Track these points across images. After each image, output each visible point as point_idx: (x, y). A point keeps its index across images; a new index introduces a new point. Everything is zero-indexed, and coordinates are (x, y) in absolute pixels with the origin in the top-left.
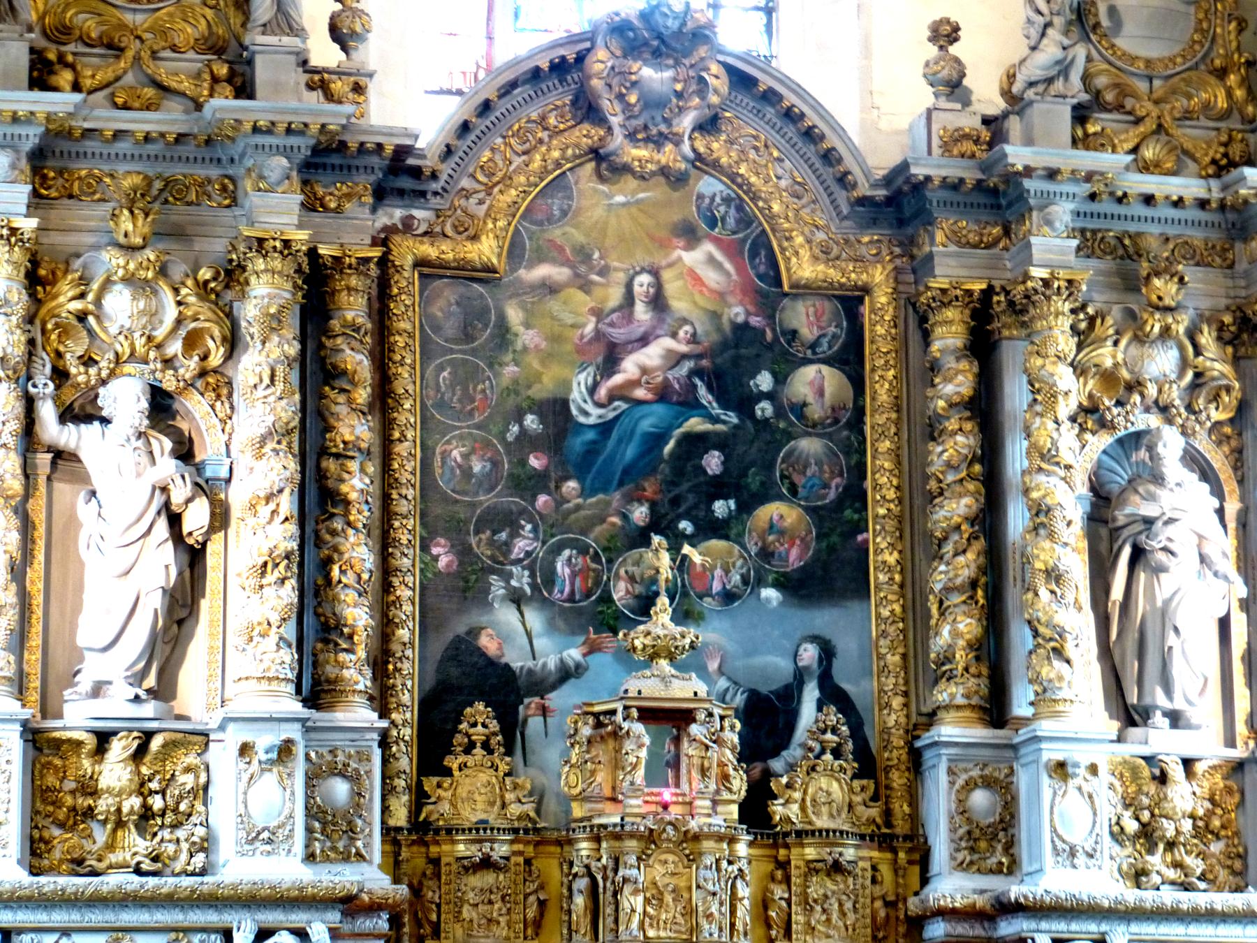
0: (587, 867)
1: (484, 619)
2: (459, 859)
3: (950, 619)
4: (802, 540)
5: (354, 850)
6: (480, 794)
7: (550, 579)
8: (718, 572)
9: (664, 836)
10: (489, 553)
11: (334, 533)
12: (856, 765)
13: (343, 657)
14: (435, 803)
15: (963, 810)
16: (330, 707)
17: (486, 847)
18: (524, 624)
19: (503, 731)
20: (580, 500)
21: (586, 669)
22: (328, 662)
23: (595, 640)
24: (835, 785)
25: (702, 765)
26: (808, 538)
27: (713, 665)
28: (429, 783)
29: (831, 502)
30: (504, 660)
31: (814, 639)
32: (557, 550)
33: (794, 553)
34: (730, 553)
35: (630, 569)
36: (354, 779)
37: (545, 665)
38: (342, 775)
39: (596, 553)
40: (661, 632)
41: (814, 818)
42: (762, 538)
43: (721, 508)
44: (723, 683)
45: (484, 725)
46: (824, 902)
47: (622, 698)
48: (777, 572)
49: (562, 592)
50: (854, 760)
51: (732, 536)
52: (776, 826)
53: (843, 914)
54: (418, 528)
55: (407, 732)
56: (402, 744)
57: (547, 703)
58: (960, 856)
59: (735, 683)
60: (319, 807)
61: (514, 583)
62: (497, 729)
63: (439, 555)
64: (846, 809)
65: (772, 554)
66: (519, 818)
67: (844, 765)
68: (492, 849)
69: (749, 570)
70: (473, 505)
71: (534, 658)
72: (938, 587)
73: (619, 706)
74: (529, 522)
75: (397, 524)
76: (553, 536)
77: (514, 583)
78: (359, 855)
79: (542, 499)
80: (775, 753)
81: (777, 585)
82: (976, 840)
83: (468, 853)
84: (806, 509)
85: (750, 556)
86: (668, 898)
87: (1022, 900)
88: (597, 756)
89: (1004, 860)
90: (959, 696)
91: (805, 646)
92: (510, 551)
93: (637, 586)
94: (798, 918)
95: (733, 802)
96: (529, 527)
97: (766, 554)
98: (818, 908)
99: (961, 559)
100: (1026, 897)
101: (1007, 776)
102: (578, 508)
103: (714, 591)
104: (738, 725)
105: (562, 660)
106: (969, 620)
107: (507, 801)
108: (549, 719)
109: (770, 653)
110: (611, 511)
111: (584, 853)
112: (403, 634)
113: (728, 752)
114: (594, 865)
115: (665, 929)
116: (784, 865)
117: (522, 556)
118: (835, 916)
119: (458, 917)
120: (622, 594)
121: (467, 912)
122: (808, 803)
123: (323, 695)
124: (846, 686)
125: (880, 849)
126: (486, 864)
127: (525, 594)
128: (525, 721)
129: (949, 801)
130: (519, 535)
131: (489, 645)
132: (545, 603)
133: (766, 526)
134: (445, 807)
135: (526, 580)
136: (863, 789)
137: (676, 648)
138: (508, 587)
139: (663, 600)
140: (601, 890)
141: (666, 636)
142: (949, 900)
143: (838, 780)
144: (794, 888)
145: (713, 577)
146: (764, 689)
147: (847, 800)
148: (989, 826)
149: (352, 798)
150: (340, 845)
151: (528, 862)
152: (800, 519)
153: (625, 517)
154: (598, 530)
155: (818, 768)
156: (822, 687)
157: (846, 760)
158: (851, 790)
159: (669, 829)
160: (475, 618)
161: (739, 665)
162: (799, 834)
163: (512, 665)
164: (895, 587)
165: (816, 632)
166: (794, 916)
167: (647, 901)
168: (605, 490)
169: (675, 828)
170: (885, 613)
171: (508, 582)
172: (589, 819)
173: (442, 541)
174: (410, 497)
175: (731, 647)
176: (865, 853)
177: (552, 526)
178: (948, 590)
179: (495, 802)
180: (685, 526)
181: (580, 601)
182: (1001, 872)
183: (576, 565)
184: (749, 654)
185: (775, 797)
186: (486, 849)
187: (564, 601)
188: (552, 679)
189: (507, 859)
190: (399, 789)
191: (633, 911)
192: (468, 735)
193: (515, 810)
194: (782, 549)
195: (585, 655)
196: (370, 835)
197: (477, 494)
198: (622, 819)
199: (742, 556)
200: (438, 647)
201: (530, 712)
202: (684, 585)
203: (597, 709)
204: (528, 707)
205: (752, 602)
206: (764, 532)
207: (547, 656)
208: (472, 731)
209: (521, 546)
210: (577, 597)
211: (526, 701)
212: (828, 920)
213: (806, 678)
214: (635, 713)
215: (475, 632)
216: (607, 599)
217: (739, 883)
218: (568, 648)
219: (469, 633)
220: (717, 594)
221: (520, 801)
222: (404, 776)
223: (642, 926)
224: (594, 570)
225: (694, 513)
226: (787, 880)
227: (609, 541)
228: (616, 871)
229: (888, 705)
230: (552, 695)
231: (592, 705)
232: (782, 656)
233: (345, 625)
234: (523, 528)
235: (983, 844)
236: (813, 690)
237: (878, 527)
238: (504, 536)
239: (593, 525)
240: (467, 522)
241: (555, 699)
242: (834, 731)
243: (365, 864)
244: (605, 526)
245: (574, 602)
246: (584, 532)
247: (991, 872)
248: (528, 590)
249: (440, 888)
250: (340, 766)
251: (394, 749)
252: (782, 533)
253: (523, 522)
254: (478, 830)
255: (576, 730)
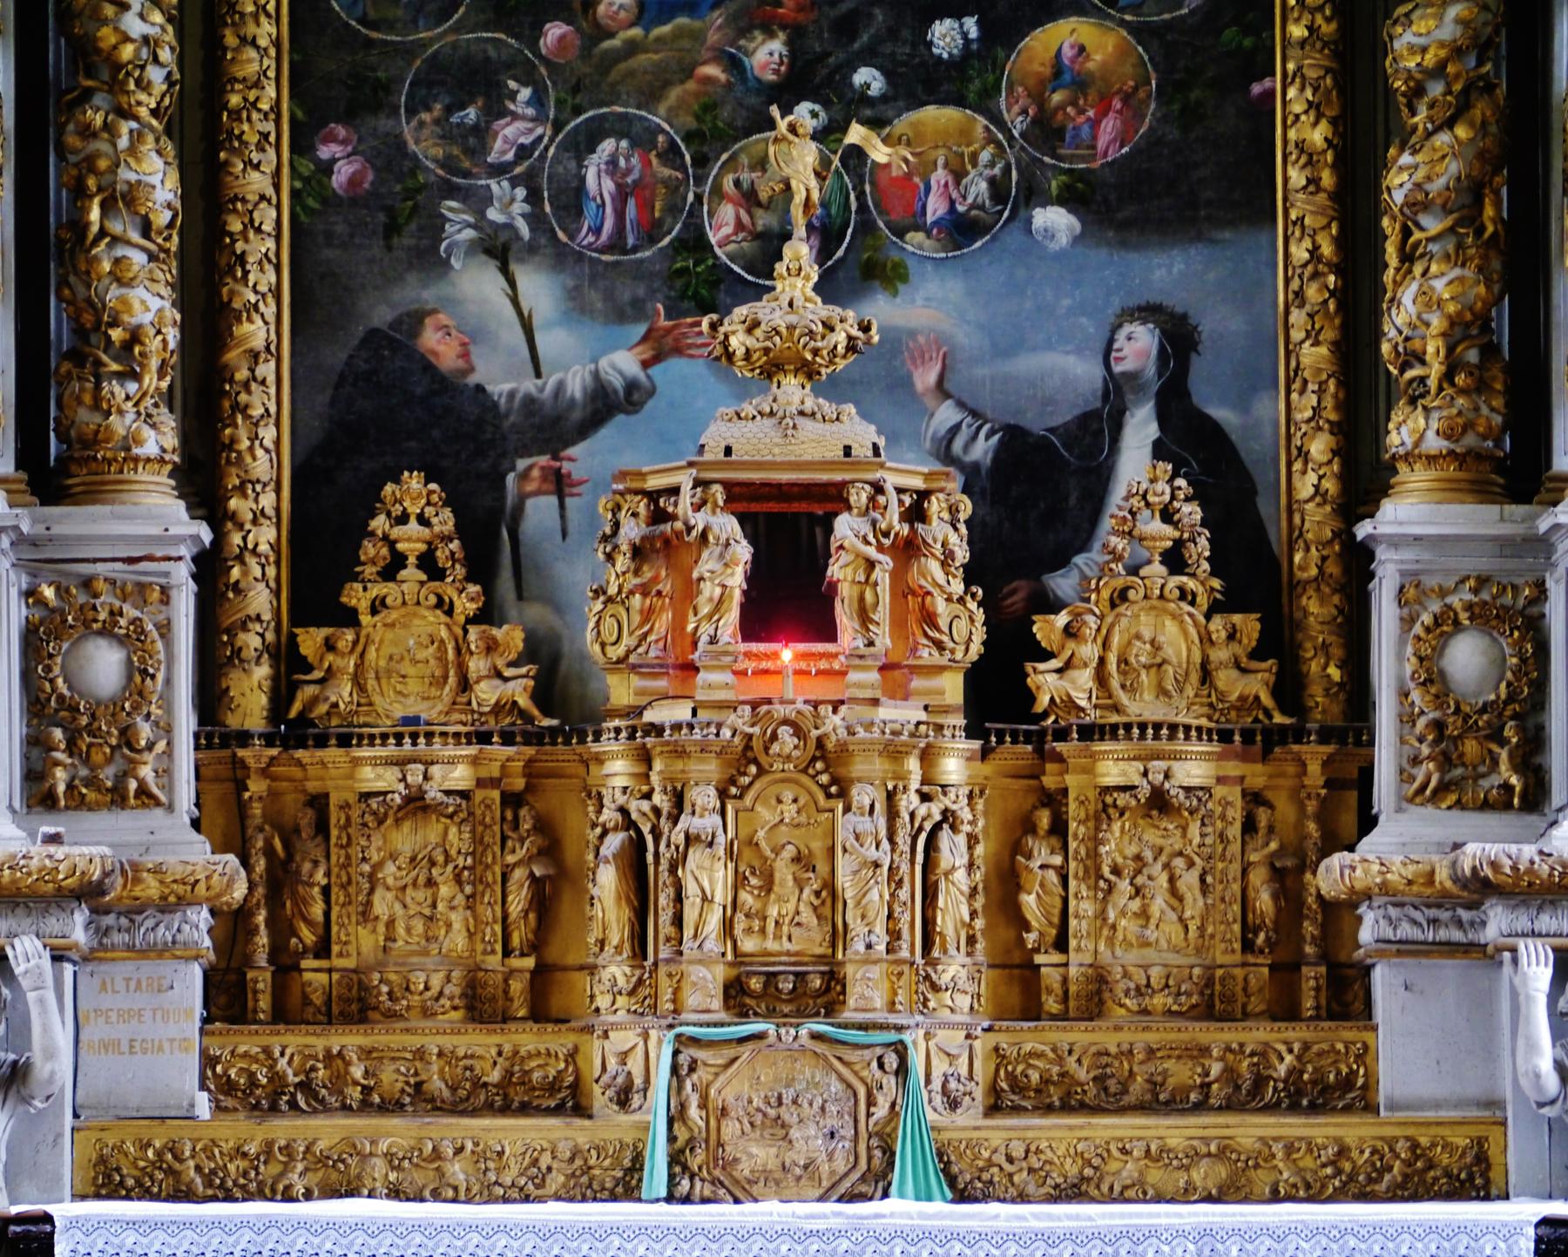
0: (623, 811)
1: (429, 295)
2: (366, 796)
3: (1418, 269)
4: (1127, 99)
5: (133, 785)
6: (415, 662)
7: (572, 199)
8: (940, 176)
9: (775, 748)
10: (439, 152)
11: (87, 132)
12: (1216, 583)
13: (117, 391)
14: (321, 682)
15: (1433, 677)
16: (92, 494)
17: (415, 774)
18: (515, 301)
19: (461, 530)
20: (636, 32)
21: (652, 392)
22: (79, 401)
23: (668, 331)
24: (1171, 627)
25: (862, 599)
26: (1142, 94)
27: (925, 378)
28: (310, 641)
29: (1192, 12)
30: (473, 379)
31: (1148, 312)
32: (584, 143)
33: (1109, 127)
34: (965, 134)
35: (746, 177)
36: (134, 639)
37: (560, 387)
38: (107, 632)
39: (673, 145)
40: (780, 320)
41: (1124, 698)
42: (1039, 99)
43: (946, 36)
44: (947, 415)
45: (423, 520)
46: (1138, 872)
47: (691, 464)
48: (1070, 171)
49: (597, 231)
50: (1213, 574)
51: (972, 96)
52: (1045, 715)
53: (1174, 891)
54: (285, 106)
55: (265, 536)
56: (252, 561)
57: (566, 466)
58: (1420, 774)
59: (975, 414)
60: (61, 698)
61: (493, 214)
62: (450, 526)
63: (334, 161)
64: (1195, 677)
65: (1060, 133)
66: (498, 709)
67: (1191, 584)
68: (426, 777)
69: (1007, 170)
70: (409, 51)
71: (538, 375)
72: (1399, 197)
73: (685, 480)
74: (525, 84)
75: (235, 100)
76: (577, 111)
77: (493, 214)
78: (143, 792)
79: (554, 31)
80: (1061, 561)
81: (1069, 199)
82: (1456, 740)
83: (380, 785)
84: (1137, 31)
85: (1011, 138)
86: (784, 872)
87: (1488, 871)
88: (655, 580)
89: (1514, 780)
90: (1431, 434)
91: (1127, 329)
92: (485, 149)
93: (759, 212)
94: (1083, 907)
95: (940, 669)
96: (525, 93)
97: (1047, 131)
98: (1124, 886)
99: (1443, 139)
100: (1494, 865)
101: (1532, 602)
102: (632, 48)
103: (930, 219)
104: (966, 508)
105: (596, 375)
106: (1457, 272)
107: (472, 676)
108: (568, 501)
109: (1049, 346)
110: (706, 54)
111: (620, 782)
112: (254, 332)
113: (934, 567)
114: (637, 807)
115: (777, 937)
116: (1054, 800)
117: (510, 156)
118: (1158, 905)
119: (366, 915)
120: (727, 230)
121: (382, 904)
122: (1112, 665)
123: (74, 468)
124: (1222, 414)
125: (1266, 755)
126: (416, 804)
127: (518, 237)
128: (519, 509)
129: (1400, 657)
130: (503, 113)
131: (441, 348)
132: (562, 257)
133: (1047, 71)
134: (342, 692)
135: (519, 207)
136: (1232, 636)
137: (816, 352)
138: (480, 223)
139: (800, 251)
140: (650, 858)
141: (791, 328)
142: (1376, 867)
143: (1174, 617)
144: (1073, 845)
145: (928, 189)
146: (1036, 422)
147: (1197, 657)
148: (1483, 710)
149: (130, 678)
150: (107, 775)
151: (512, 800)
152: (1123, 52)
153: (734, 65)
154: (674, 94)
155: (1131, 594)
156: (1163, 418)
157: (1193, 575)
158: (1206, 639)
159: (785, 732)
160: (414, 292)
161: (979, 375)
162: (1089, 733)
163: (489, 388)
164: (1322, 198)
165: (1155, 298)
166: (1072, 903)
167: (739, 882)
168: (692, 9)
169: (799, 732)
170: (1300, 253)
171: (481, 214)
172: (638, 711)
173: (341, 131)
174: (263, 42)
175: (965, 337)
176: (1233, 768)
177: (576, 90)
178: (1418, 204)
179: (446, 677)
180: (868, 78)
181: (635, 249)
182: (1507, 806)
183: (629, 171)
184: (1005, 349)
185: (1047, 655)
186: (415, 774)
187: (602, 251)
188: (577, 415)
189: (465, 795)
190: (249, 654)
191: (706, 899)
192: (391, 543)
193: (487, 693)
194: (1081, 119)
195: (646, 365)
196: (169, 752)
197: (414, 25)
198: (694, 713)
199: (991, 140)
200: (336, 356)
201: (531, 487)
202: (863, 208)
203: (653, 483)
204: (524, 476)
205: (1013, 237)
206: (1042, 83)
207: (567, 369)
208: (396, 532)
209: (509, 135)
210: (631, 241)
211: (522, 464)
212: (1144, 914)
213: (1129, 397)
214: (718, 492)
215: (415, 320)
216: (695, 242)
217: (945, 835)
218: (614, 348)
219: (396, 324)
220: (935, 223)
221: (498, 675)
222: (258, 628)
223: (728, 927)
224: (666, 182)
225: (887, 48)
226: (1059, 829)
227: (698, 118)
228: (675, 820)
229: (1304, 454)
230: (572, 451)
231: (642, 476)
232: (1079, 351)
233: (115, 323)
234: (513, 96)
235: (1471, 747)
236: (1145, 422)
237: (1291, 66)
238: (471, 114)
239: (667, 84)
240: (386, 88)
241: (583, 458)
242: (1167, 516)
243: (159, 812)
244: (691, 85)
245: (625, 252)
246: (650, 97)
247: (1486, 806)
248: (524, 230)
249: (328, 857)
250: (103, 616)
251: (236, 573)
252: (1081, 84)
253: (512, 84)
254: (399, 738)
255: (616, 525)
